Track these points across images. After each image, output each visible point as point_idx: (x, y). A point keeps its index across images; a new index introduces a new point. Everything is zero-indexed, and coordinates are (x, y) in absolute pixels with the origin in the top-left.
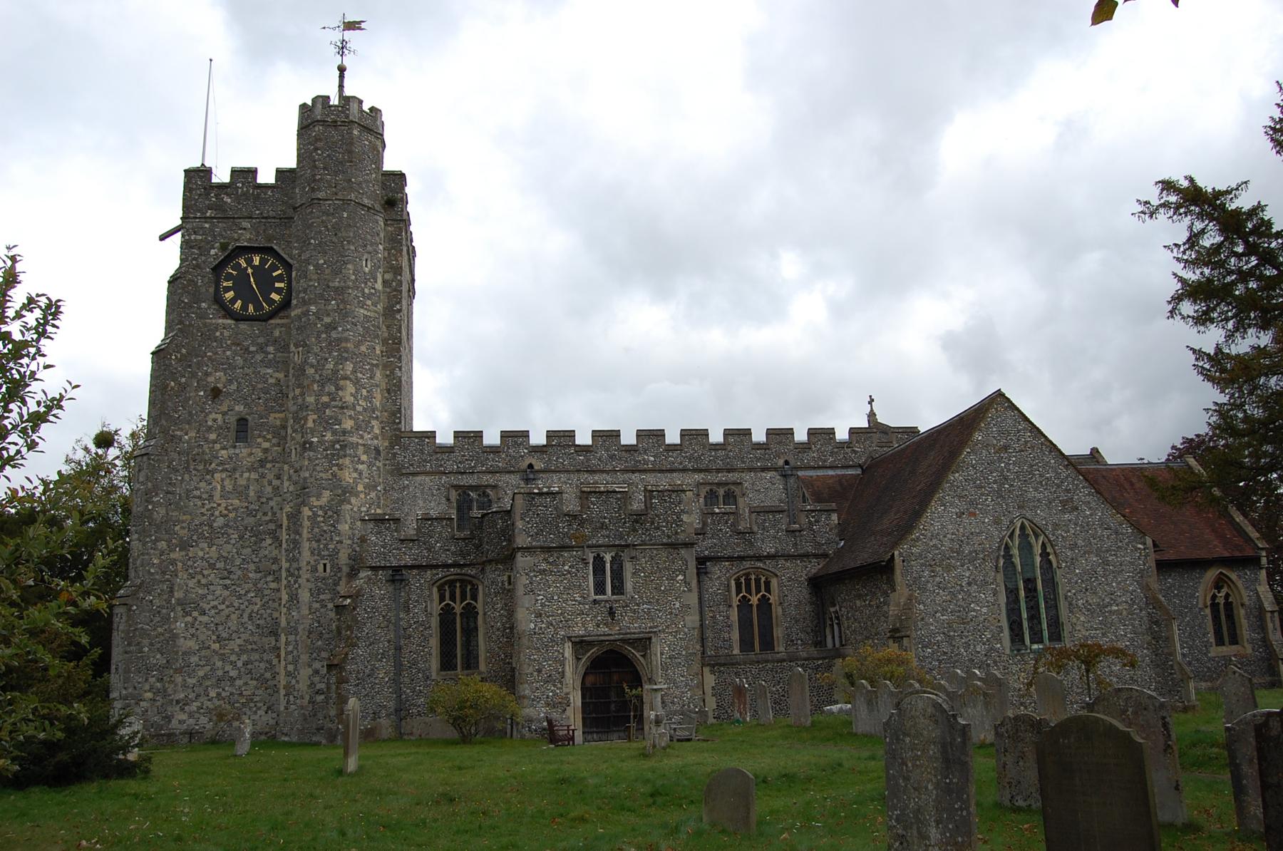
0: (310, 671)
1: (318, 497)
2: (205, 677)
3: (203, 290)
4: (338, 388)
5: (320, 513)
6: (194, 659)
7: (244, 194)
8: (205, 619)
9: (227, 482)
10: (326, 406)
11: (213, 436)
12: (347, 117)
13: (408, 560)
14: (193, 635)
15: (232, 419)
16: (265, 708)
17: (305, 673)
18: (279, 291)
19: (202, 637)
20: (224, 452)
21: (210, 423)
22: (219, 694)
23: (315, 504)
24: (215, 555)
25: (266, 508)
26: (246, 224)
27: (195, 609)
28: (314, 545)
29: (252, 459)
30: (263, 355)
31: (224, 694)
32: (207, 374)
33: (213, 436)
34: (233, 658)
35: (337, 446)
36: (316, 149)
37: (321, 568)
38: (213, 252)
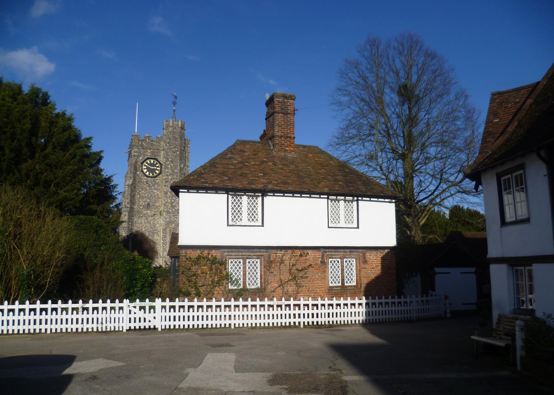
3: (138, 168)
7: (149, 142)
11: (141, 208)
12: (178, 126)
15: (146, 203)
18: (158, 170)
20: (144, 212)
21: (141, 204)
25: (155, 226)
26: (149, 151)
29: (151, 214)
30: (154, 187)
32: (140, 191)
33: (141, 208)
36: (170, 134)
38: (140, 158)
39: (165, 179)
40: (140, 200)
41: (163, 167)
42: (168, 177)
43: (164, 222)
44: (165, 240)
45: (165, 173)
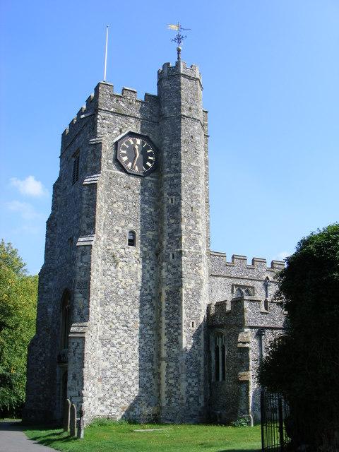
0: (186, 384)
1: (189, 283)
2: (115, 385)
4: (197, 223)
5: (190, 293)
6: (108, 373)
8: (114, 349)
9: (125, 268)
10: (191, 231)
13: (264, 324)
14: (107, 359)
16: (146, 404)
17: (184, 385)
19: (113, 361)
22: (122, 395)
23: (189, 287)
24: (119, 311)
27: (109, 343)
28: (188, 311)
31: (125, 395)
33: (117, 240)
34: (130, 374)
35: (198, 256)
37: (191, 324)
39: (172, 179)
40: (114, 223)
41: (165, 154)
42: (177, 175)
43: (170, 276)
44: (173, 317)
45: (169, 167)
